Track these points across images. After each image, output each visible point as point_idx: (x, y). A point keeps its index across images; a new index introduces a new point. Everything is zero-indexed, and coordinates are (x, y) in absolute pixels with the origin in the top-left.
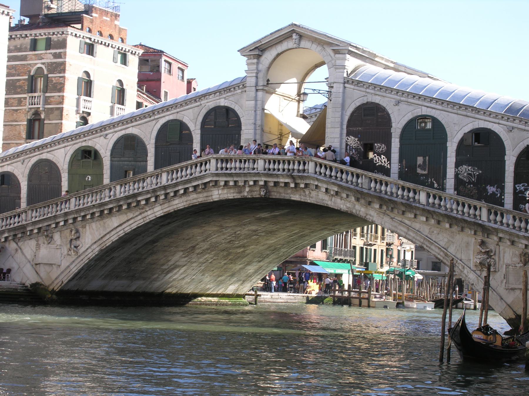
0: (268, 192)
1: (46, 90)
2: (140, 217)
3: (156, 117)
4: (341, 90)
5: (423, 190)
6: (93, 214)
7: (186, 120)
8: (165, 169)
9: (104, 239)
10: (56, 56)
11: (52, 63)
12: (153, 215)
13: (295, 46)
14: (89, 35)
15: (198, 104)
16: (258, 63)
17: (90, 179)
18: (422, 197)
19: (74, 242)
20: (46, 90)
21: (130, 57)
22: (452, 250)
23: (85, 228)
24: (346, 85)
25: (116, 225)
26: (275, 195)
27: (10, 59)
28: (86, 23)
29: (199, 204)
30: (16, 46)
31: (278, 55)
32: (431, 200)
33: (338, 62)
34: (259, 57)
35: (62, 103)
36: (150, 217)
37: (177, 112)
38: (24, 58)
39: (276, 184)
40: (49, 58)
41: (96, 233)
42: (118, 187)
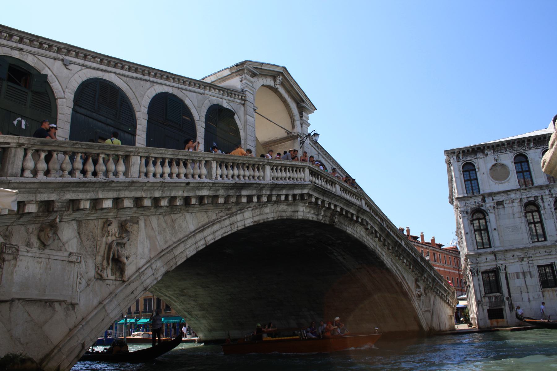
2: (227, 222)
3: (152, 79)
7: (188, 102)
9: (177, 252)
12: (243, 223)
15: (202, 91)
17: (23, 126)
23: (137, 223)
25: (192, 228)
29: (287, 219)
36: (239, 224)
37: (178, 88)
41: (158, 238)
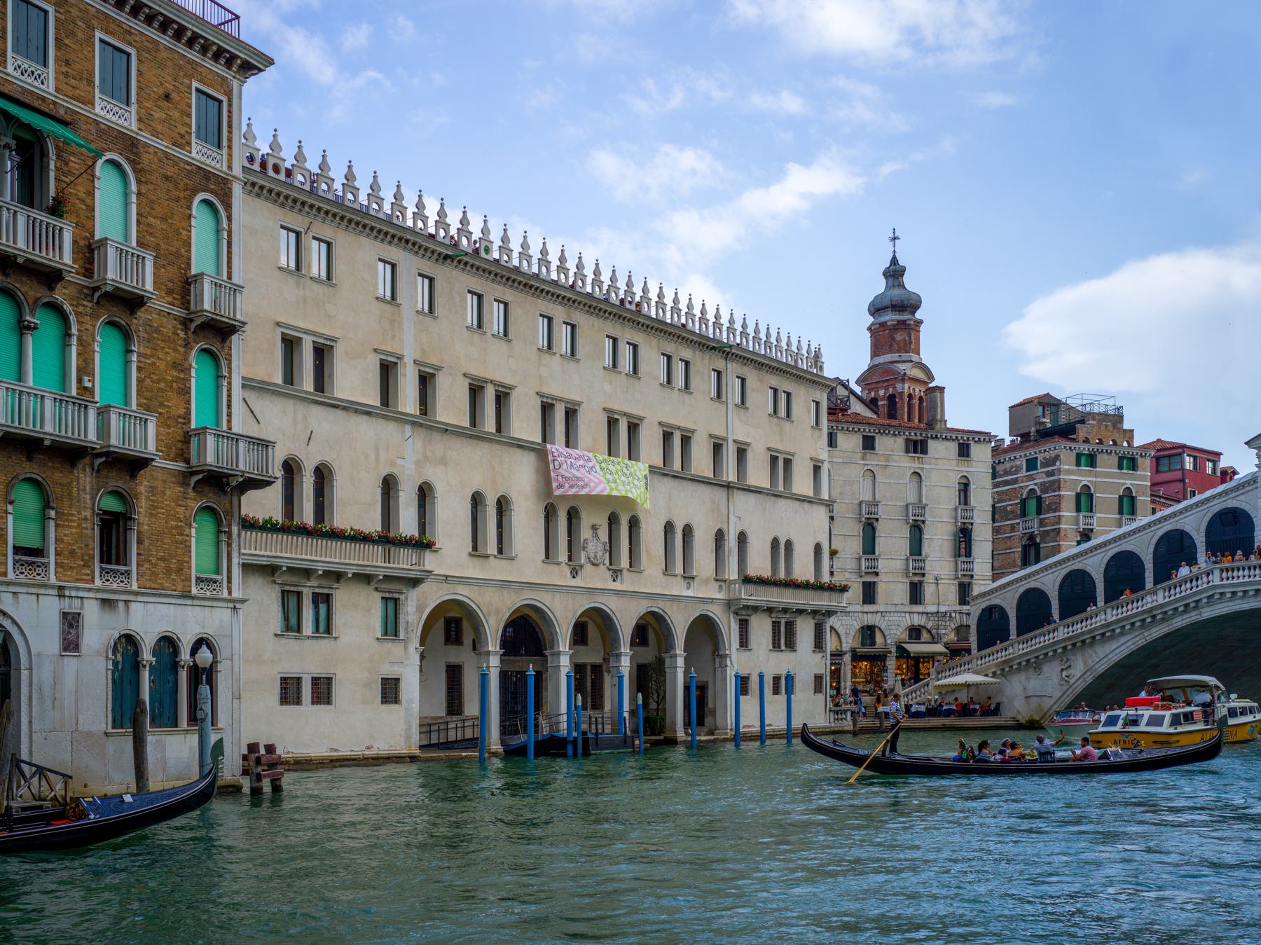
1: (1039, 512)
10: (1049, 474)
11: (1045, 483)
20: (1039, 512)
21: (1140, 460)
27: (996, 486)
30: (1005, 471)
35: (1059, 523)
38: (1015, 481)
40: (1040, 476)
42: (1109, 611)
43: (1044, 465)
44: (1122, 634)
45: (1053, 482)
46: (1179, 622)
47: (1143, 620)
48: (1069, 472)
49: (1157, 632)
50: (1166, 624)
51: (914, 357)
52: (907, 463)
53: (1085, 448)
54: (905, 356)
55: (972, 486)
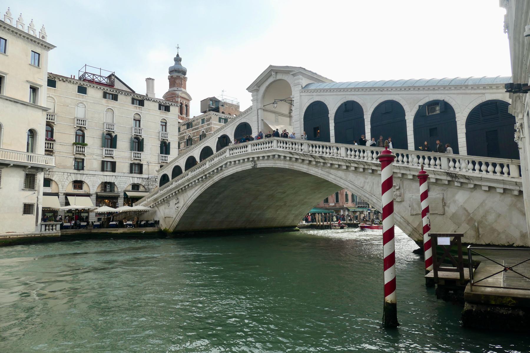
0: (255, 165)
4: (298, 98)
5: (342, 147)
6: (182, 189)
8: (207, 159)
13: (274, 79)
14: (223, 115)
16: (257, 95)
18: (342, 151)
19: (177, 206)
22: (367, 188)
24: (301, 94)
26: (259, 166)
28: (221, 109)
31: (268, 87)
32: (349, 152)
33: (296, 82)
34: (257, 91)
38: (198, 128)
39: (258, 158)
43: (207, 121)
44: (196, 185)
45: (209, 128)
46: (216, 178)
47: (202, 177)
48: (215, 124)
49: (209, 183)
50: (211, 180)
51: (183, 90)
52: (134, 109)
53: (223, 116)
54: (179, 89)
55: (168, 124)
